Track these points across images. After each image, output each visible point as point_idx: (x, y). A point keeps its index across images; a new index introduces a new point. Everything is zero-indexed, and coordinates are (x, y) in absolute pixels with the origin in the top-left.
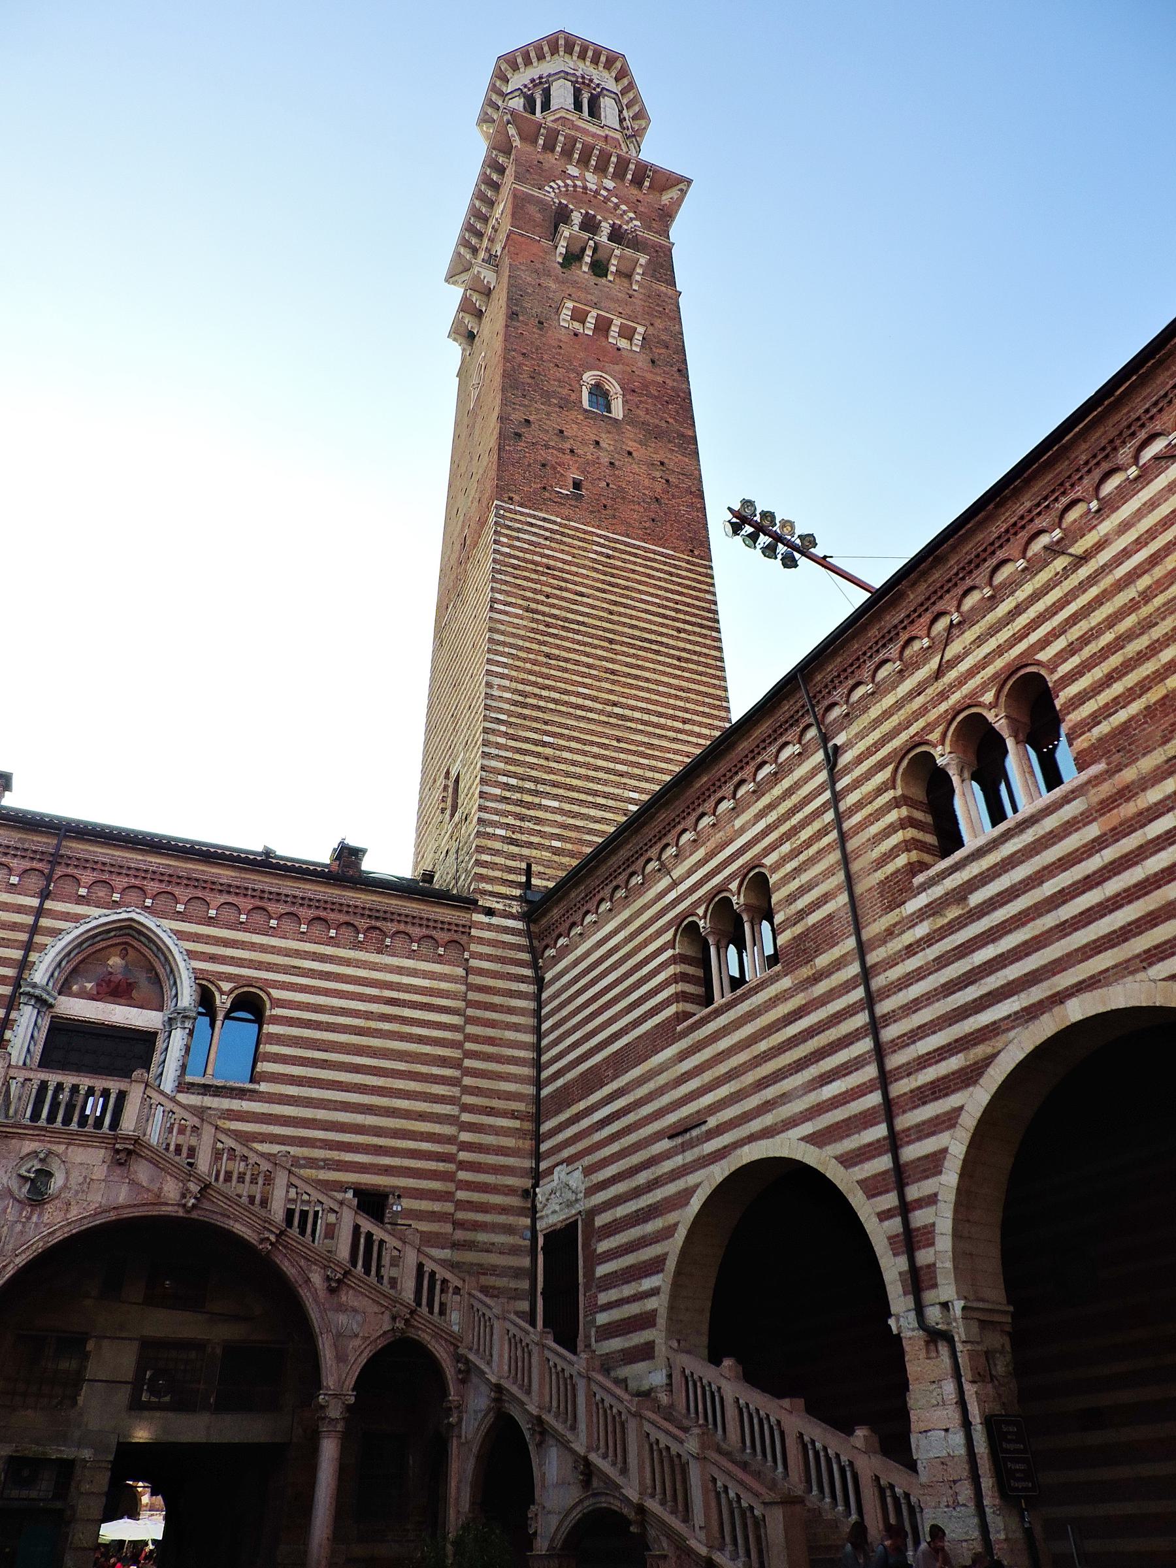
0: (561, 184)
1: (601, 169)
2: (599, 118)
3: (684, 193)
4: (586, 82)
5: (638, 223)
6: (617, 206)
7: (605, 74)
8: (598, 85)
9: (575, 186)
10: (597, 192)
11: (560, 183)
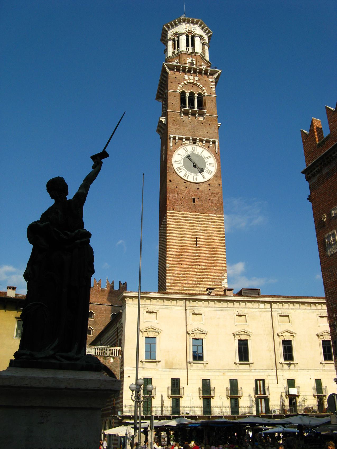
0: (182, 83)
4: (190, 32)
7: (196, 26)
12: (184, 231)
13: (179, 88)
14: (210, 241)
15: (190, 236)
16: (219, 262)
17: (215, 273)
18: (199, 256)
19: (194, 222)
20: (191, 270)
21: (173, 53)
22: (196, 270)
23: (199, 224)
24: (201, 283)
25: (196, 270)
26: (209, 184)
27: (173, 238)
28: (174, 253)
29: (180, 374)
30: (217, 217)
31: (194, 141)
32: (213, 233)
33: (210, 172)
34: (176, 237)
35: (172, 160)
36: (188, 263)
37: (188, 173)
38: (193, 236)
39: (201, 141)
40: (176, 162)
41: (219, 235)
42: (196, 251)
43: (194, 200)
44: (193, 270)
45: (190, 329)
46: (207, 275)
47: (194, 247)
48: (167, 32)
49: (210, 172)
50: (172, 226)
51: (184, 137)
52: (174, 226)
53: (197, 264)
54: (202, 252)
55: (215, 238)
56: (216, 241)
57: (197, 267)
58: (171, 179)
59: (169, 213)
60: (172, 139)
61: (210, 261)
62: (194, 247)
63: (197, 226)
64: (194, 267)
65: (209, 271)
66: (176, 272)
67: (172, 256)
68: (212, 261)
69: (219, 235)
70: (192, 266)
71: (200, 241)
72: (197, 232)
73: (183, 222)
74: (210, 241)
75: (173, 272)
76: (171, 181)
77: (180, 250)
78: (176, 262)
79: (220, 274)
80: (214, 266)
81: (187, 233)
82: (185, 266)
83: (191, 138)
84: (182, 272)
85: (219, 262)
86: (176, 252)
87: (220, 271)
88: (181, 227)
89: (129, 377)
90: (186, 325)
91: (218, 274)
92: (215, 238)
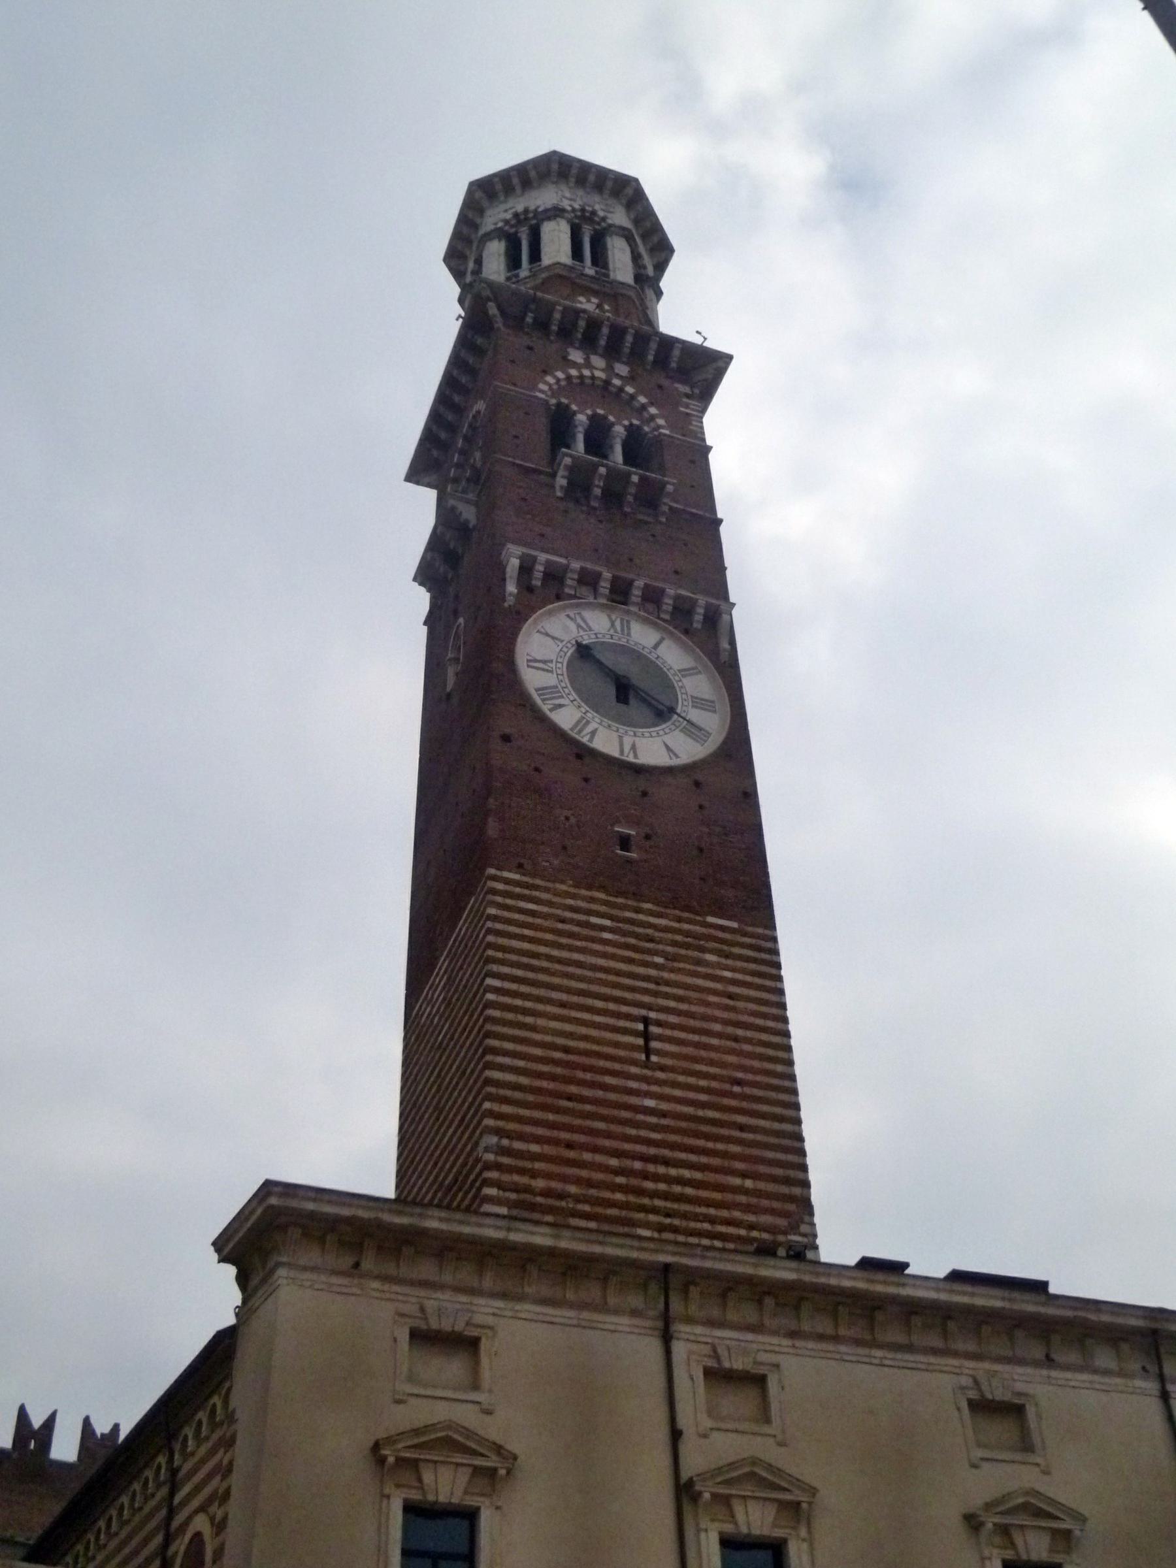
0: (560, 375)
1: (612, 352)
2: (605, 266)
3: (719, 374)
5: (661, 422)
6: (633, 397)
8: (604, 219)
9: (581, 377)
10: (607, 383)
11: (560, 375)
12: (581, 979)
13: (542, 386)
14: (715, 1041)
15: (612, 1006)
16: (770, 1155)
18: (664, 1114)
20: (620, 1180)
21: (508, 279)
22: (649, 1185)
23: (656, 953)
25: (649, 1185)
26: (697, 784)
27: (518, 1002)
28: (524, 1080)
30: (745, 934)
31: (620, 594)
32: (727, 1008)
33: (693, 730)
34: (539, 999)
35: (511, 653)
36: (607, 1143)
37: (595, 721)
38: (624, 1009)
39: (652, 597)
40: (531, 662)
41: (760, 1022)
42: (644, 1087)
43: (625, 842)
44: (634, 1182)
45: (694, 1461)
46: (712, 1221)
47: (634, 1063)
48: (481, 212)
50: (515, 944)
51: (576, 565)
52: (526, 946)
53: (652, 1151)
54: (678, 1093)
55: (740, 1032)
56: (747, 1047)
57: (651, 1168)
58: (508, 731)
59: (494, 878)
60: (515, 563)
61: (720, 1146)
63: (646, 964)
64: (638, 1165)
65: (717, 1196)
66: (540, 1183)
67: (518, 1095)
68: (735, 1149)
69: (760, 1022)
70: (628, 1163)
71: (660, 1038)
72: (646, 991)
73: (571, 935)
74: (715, 1041)
75: (524, 1180)
76: (506, 738)
77: (559, 1070)
78: (540, 1131)
79: (782, 1222)
80: (744, 1175)
81: (594, 988)
82: (587, 1156)
83: (607, 575)
84: (573, 1189)
85: (770, 1155)
86: (540, 1075)
87: (776, 1205)
88: (565, 954)
90: (676, 1435)
92: (740, 1032)
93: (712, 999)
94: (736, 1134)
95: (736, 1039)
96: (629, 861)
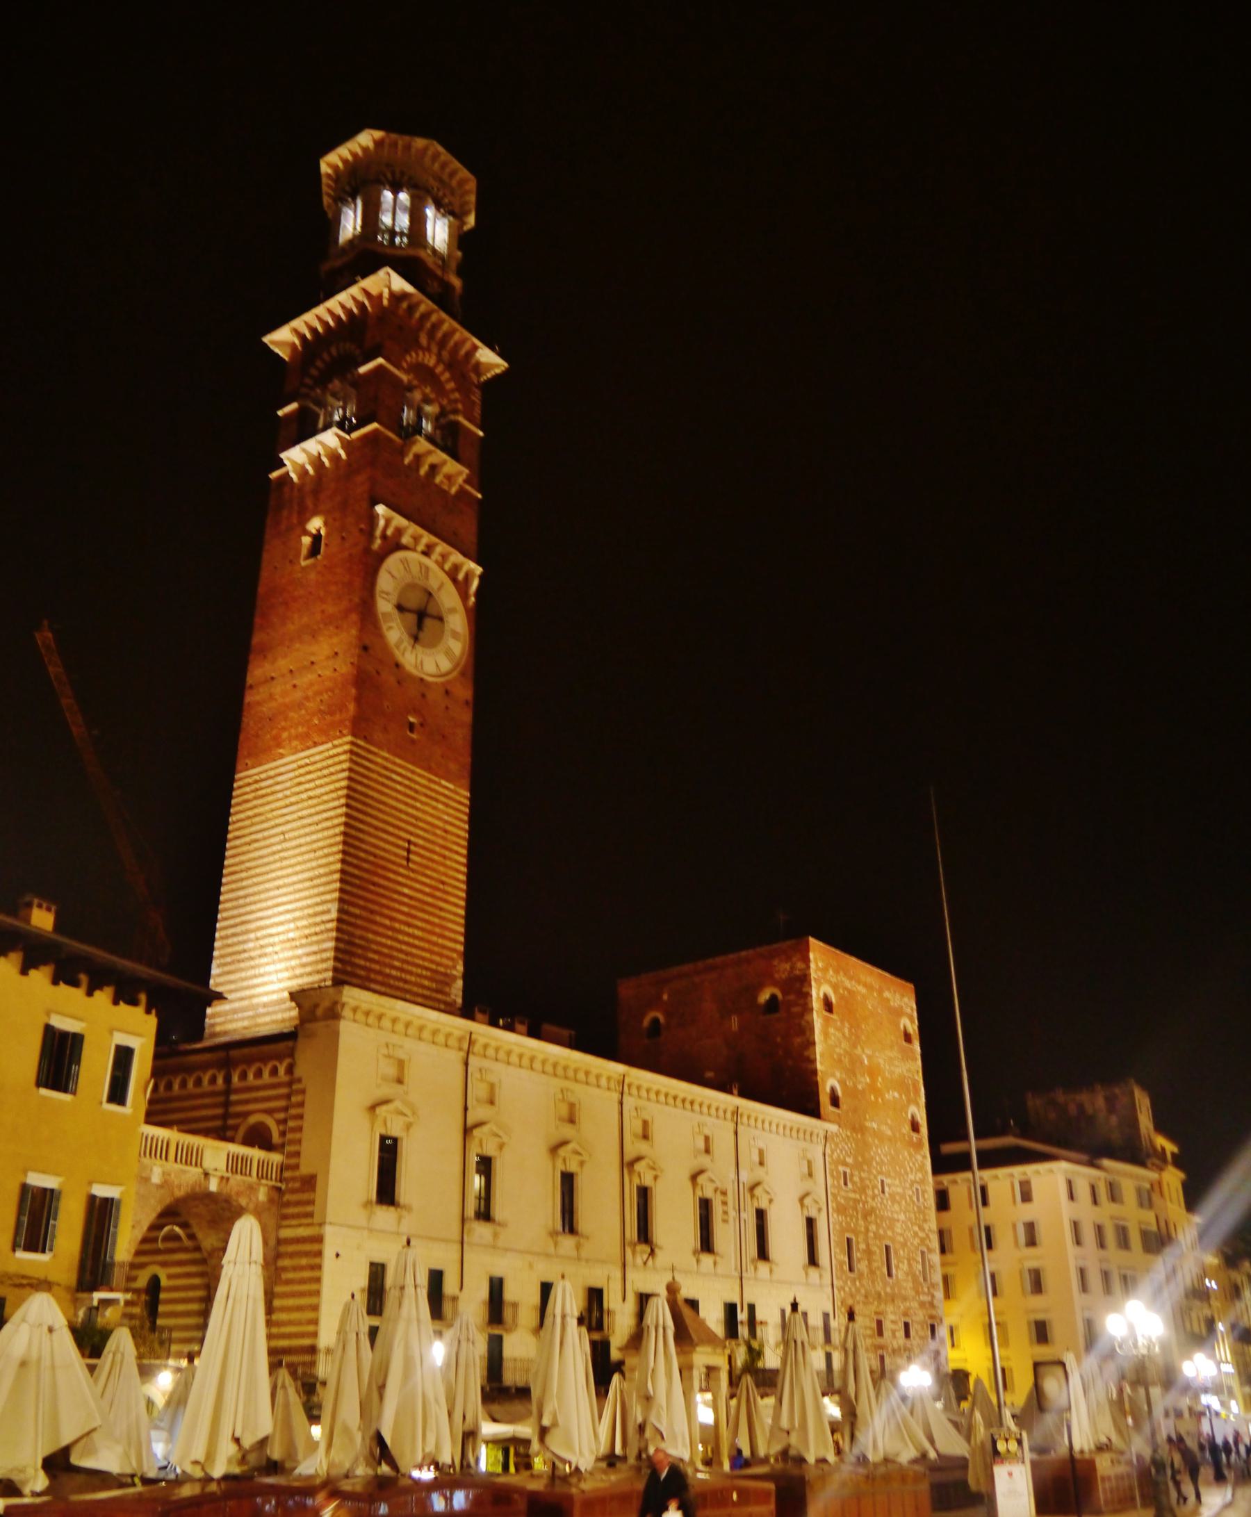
14: (436, 857)
17: (441, 955)
18: (411, 898)
19: (409, 792)
24: (408, 977)
29: (444, 1257)
43: (411, 727)
47: (401, 866)
49: (448, 653)
62: (401, 866)
68: (436, 920)
74: (436, 857)
89: (338, 1255)
90: (466, 1109)
91: (445, 961)
92: (447, 853)
93: (439, 832)
94: (437, 912)
95: (444, 857)
96: (413, 742)
